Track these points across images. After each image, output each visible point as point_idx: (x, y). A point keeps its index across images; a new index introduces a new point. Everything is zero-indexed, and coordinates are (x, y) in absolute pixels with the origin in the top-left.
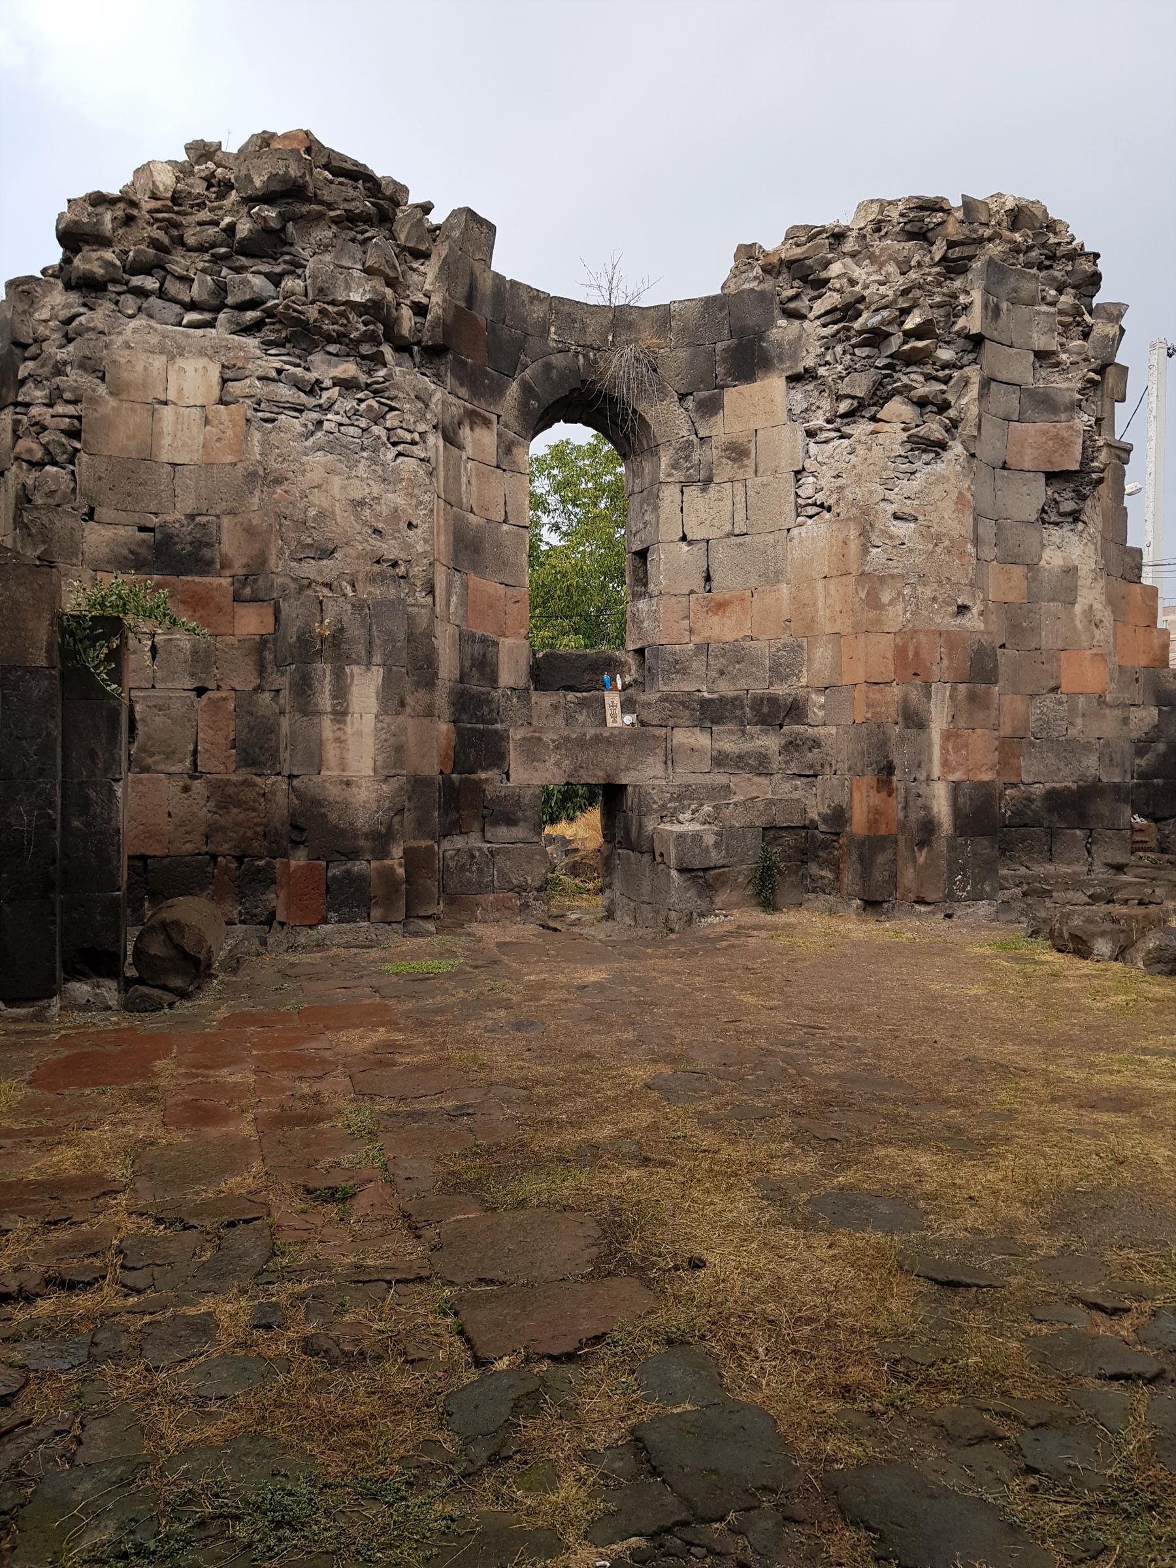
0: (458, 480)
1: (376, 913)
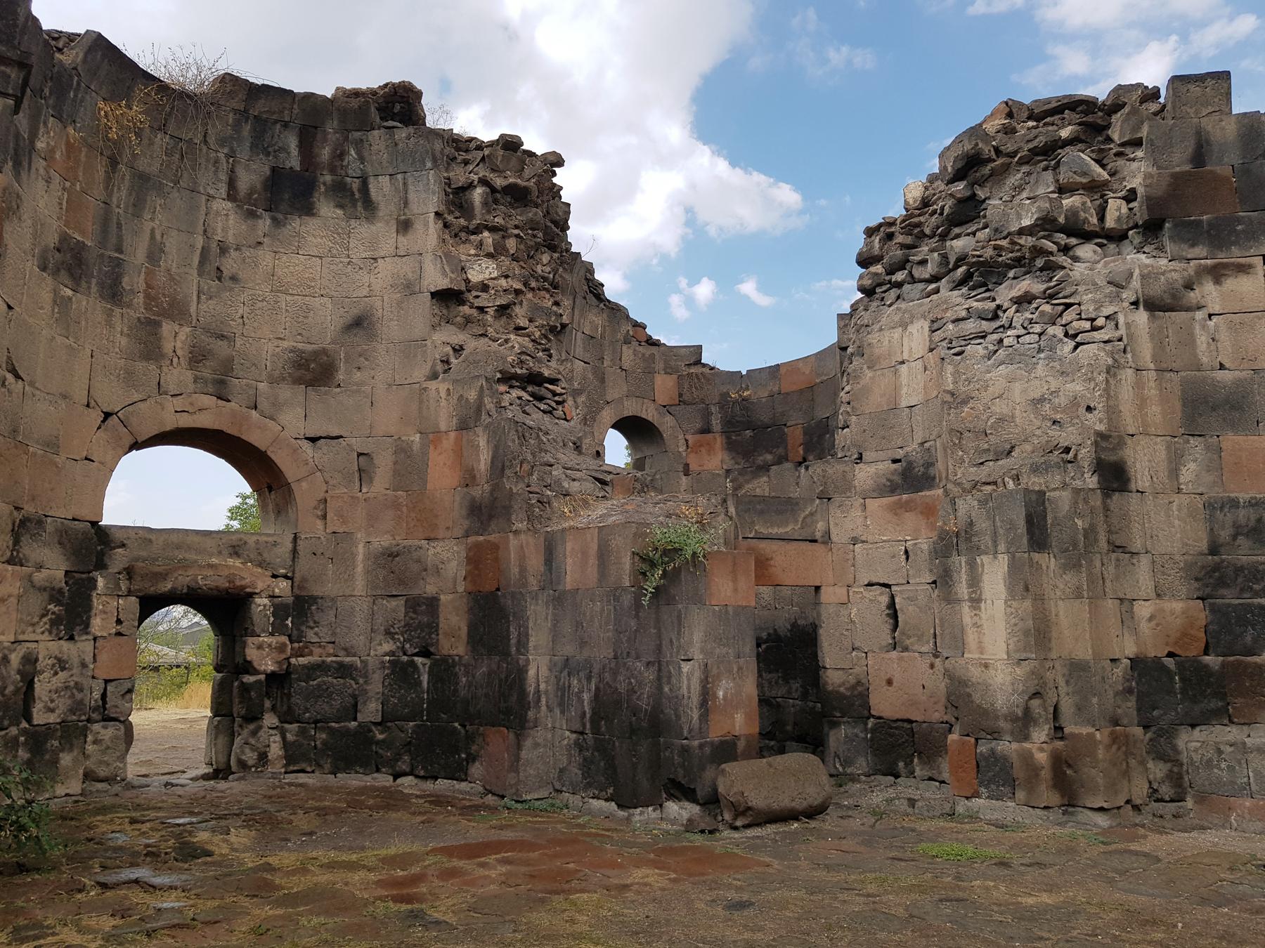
0: (1191, 341)
1: (1021, 795)
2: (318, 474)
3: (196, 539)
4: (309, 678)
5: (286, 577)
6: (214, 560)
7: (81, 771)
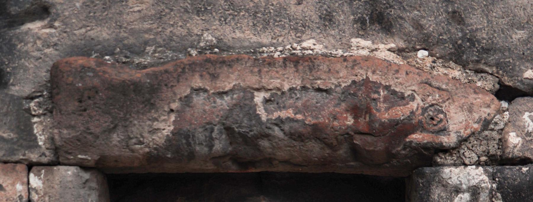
6: (312, 45)
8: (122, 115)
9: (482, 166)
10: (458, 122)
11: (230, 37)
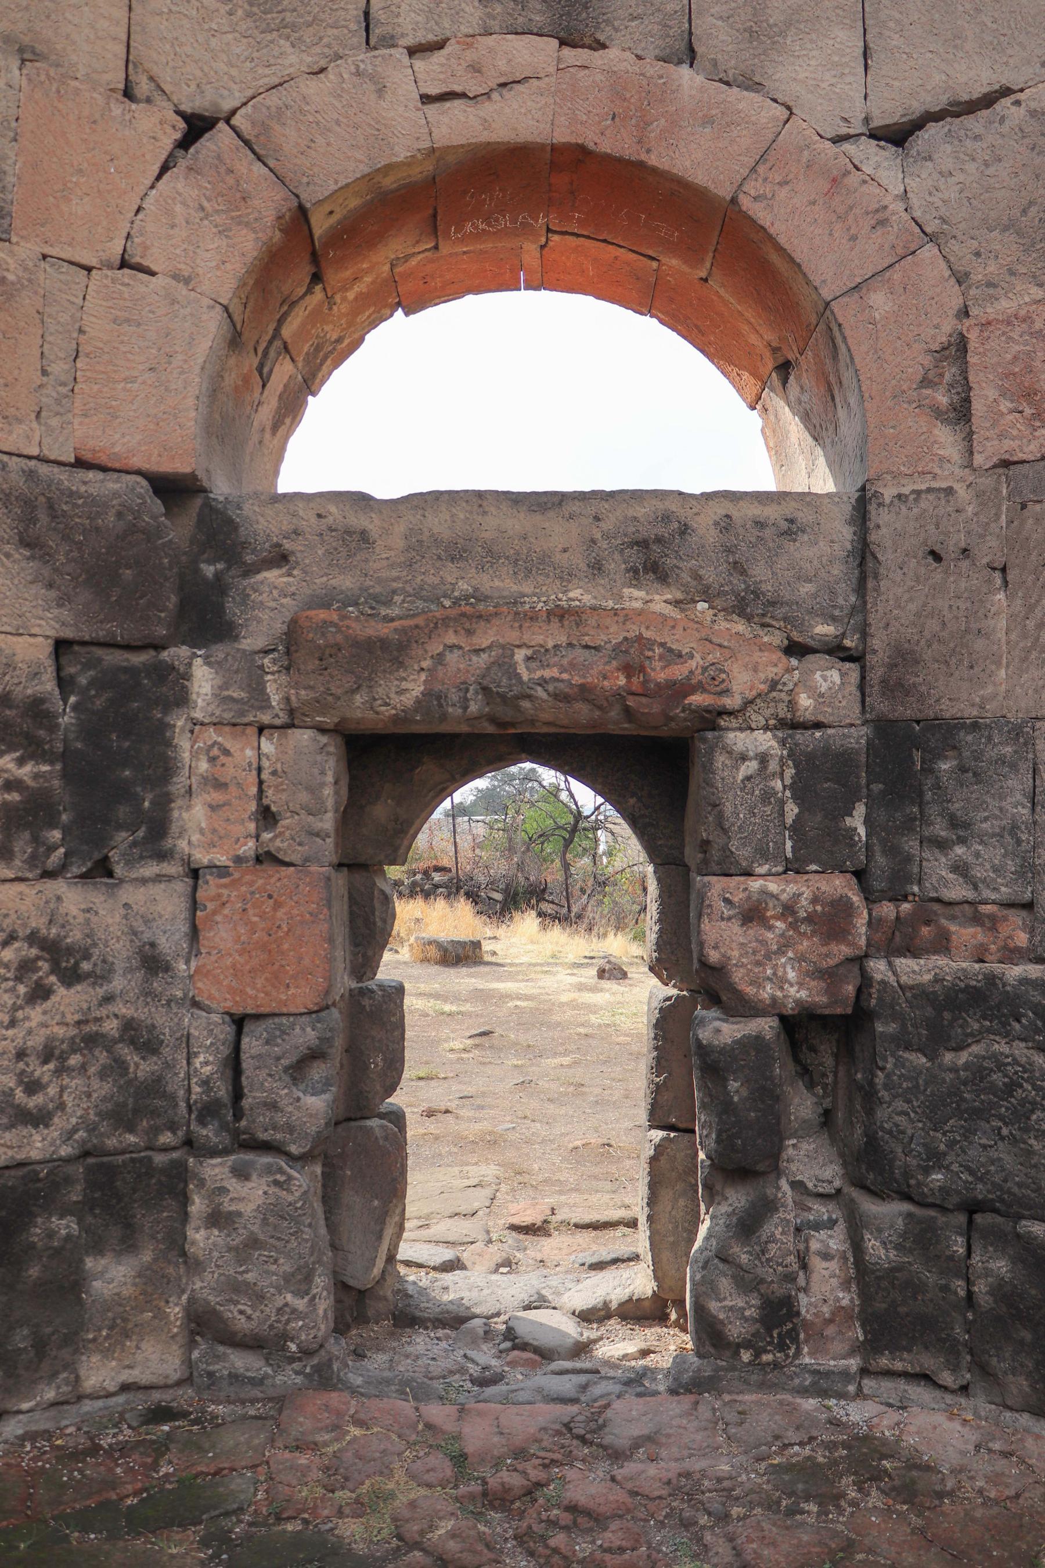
2: (929, 251)
3: (516, 523)
4: (937, 1039)
5: (837, 651)
6: (579, 595)
7: (175, 1311)
8: (366, 674)
9: (771, 730)
10: (742, 682)
11: (487, 586)
